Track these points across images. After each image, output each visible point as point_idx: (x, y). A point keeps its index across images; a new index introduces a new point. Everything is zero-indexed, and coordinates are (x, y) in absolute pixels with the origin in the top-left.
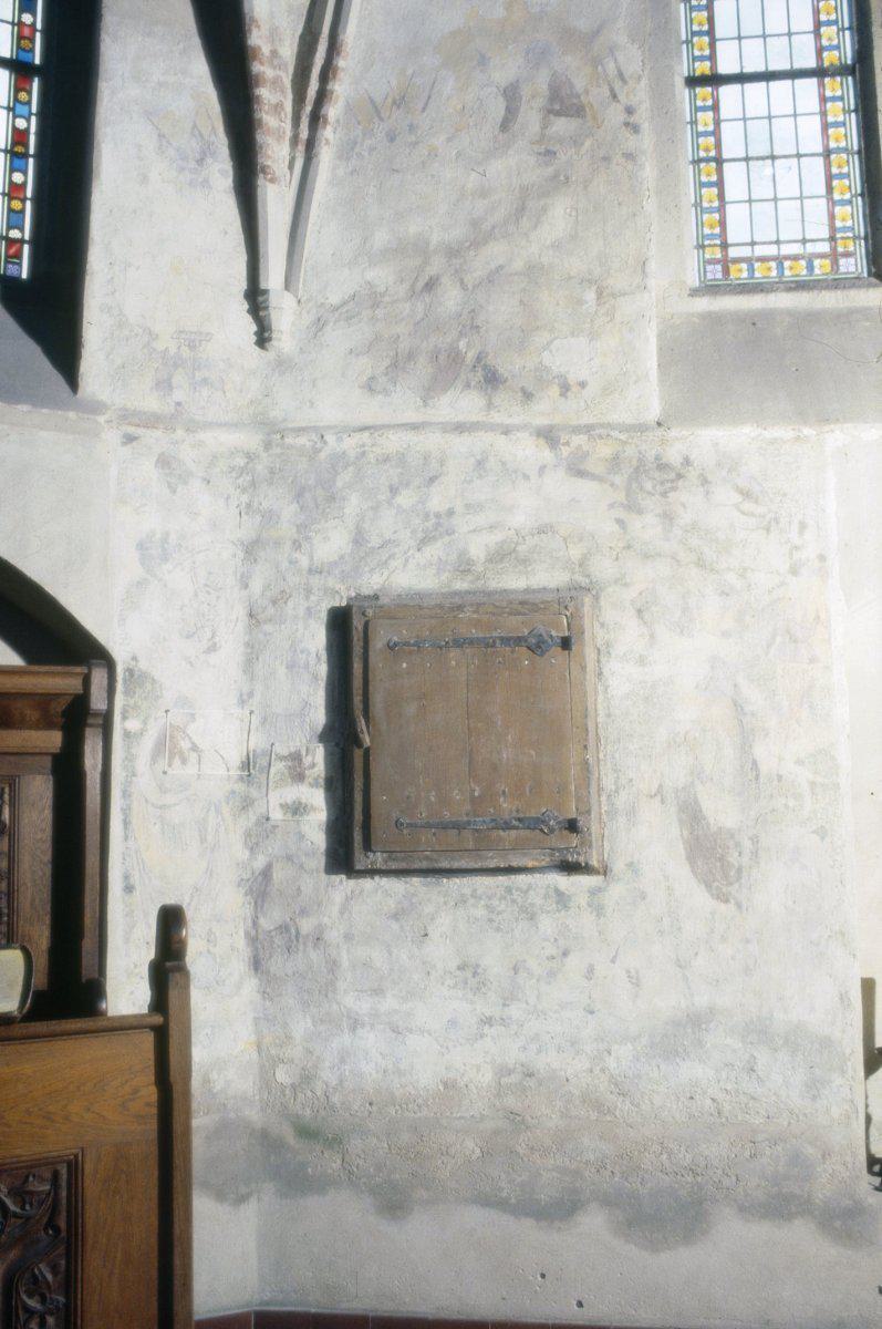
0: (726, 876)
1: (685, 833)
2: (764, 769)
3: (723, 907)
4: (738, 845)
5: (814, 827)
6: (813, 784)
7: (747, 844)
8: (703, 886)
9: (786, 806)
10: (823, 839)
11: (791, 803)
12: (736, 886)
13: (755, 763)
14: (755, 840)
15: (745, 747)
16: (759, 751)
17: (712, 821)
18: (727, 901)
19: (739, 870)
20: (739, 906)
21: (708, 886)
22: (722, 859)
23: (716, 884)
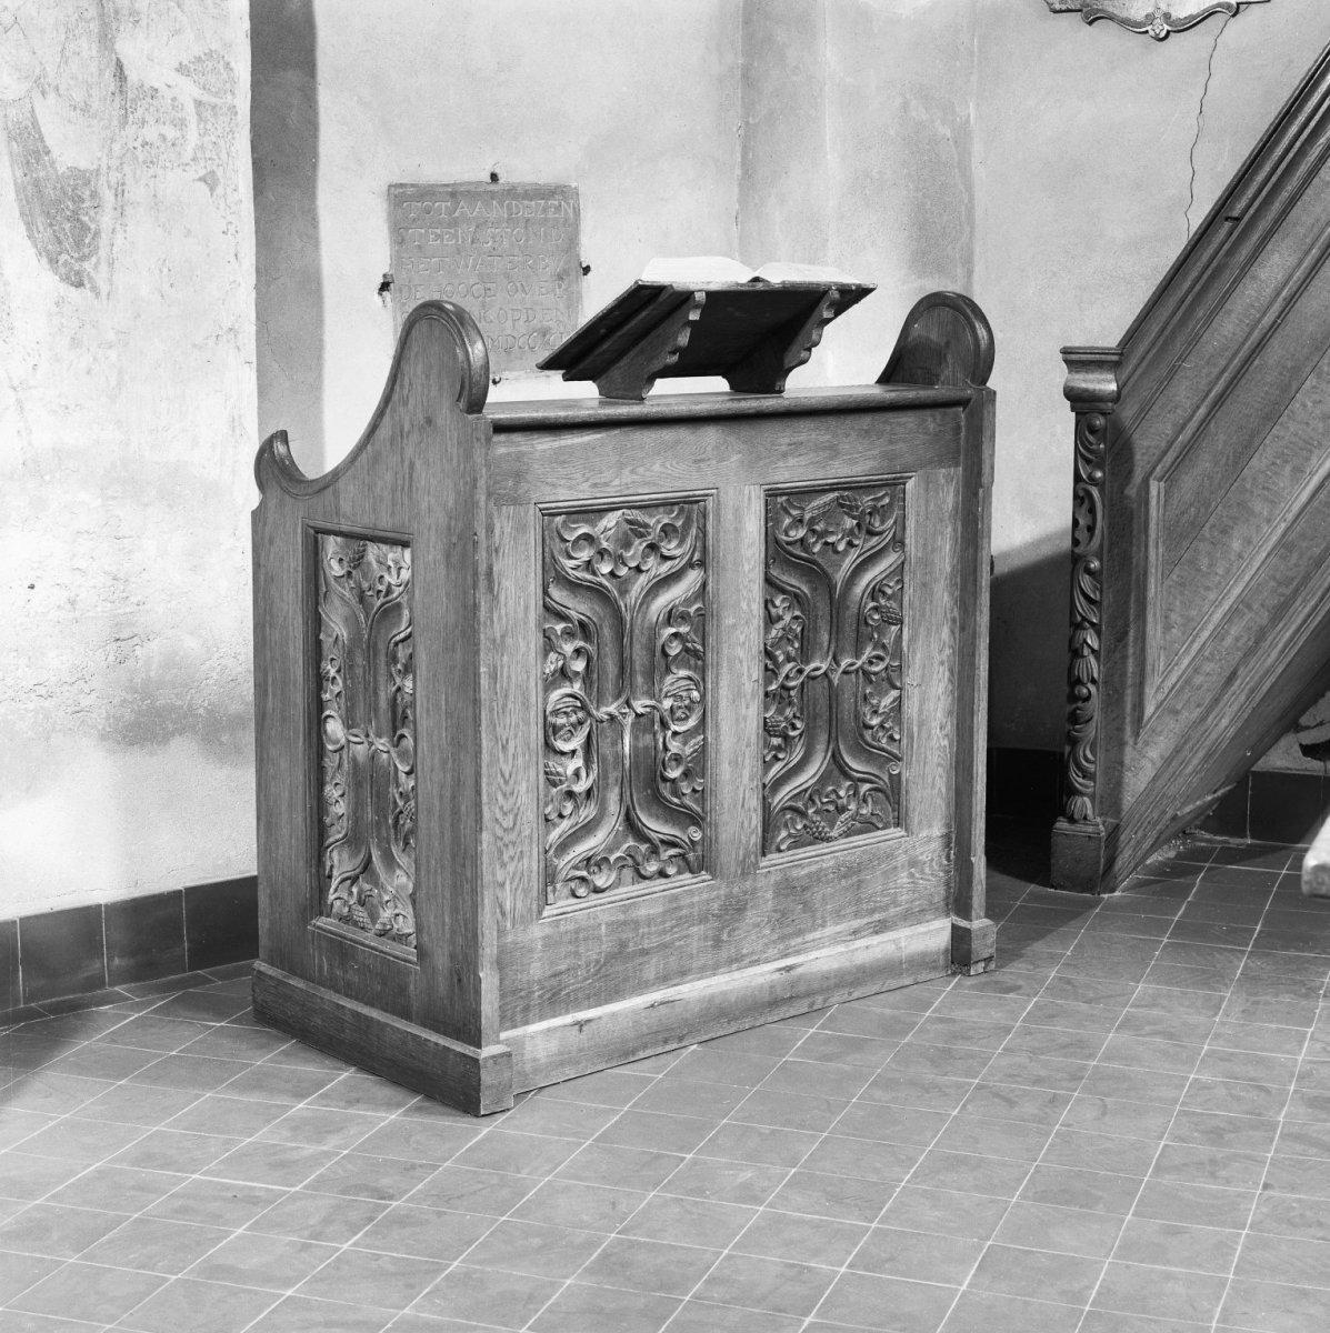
0: (78, 244)
1: (19, 173)
2: (132, 75)
3: (73, 293)
4: (94, 195)
5: (202, 173)
6: (199, 104)
7: (108, 196)
8: (44, 260)
9: (164, 138)
10: (212, 190)
11: (171, 133)
12: (94, 259)
13: (120, 66)
14: (120, 191)
15: (106, 39)
16: (130, 48)
17: (55, 153)
18: (80, 284)
19: (97, 234)
20: (96, 291)
21: (53, 261)
22: (75, 218)
23: (64, 257)
